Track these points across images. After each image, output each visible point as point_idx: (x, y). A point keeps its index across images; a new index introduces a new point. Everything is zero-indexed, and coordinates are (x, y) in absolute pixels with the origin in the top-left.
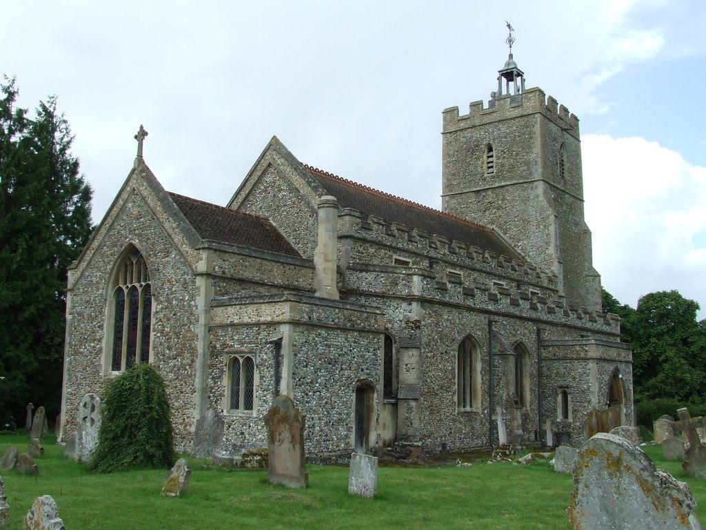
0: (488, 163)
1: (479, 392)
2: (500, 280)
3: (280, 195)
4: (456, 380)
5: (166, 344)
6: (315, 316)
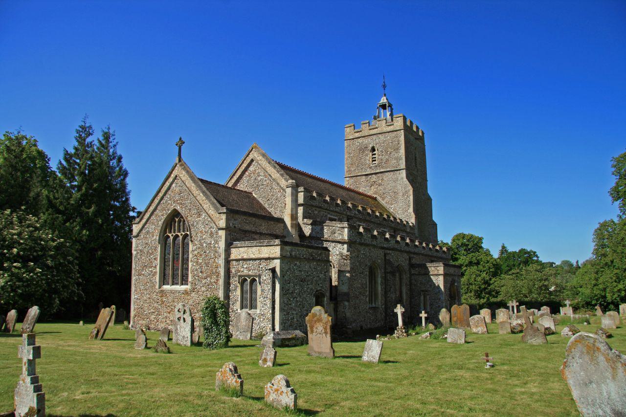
0: (372, 158)
1: (380, 298)
2: (385, 228)
3: (259, 179)
4: (368, 289)
5: (199, 270)
6: (293, 253)
